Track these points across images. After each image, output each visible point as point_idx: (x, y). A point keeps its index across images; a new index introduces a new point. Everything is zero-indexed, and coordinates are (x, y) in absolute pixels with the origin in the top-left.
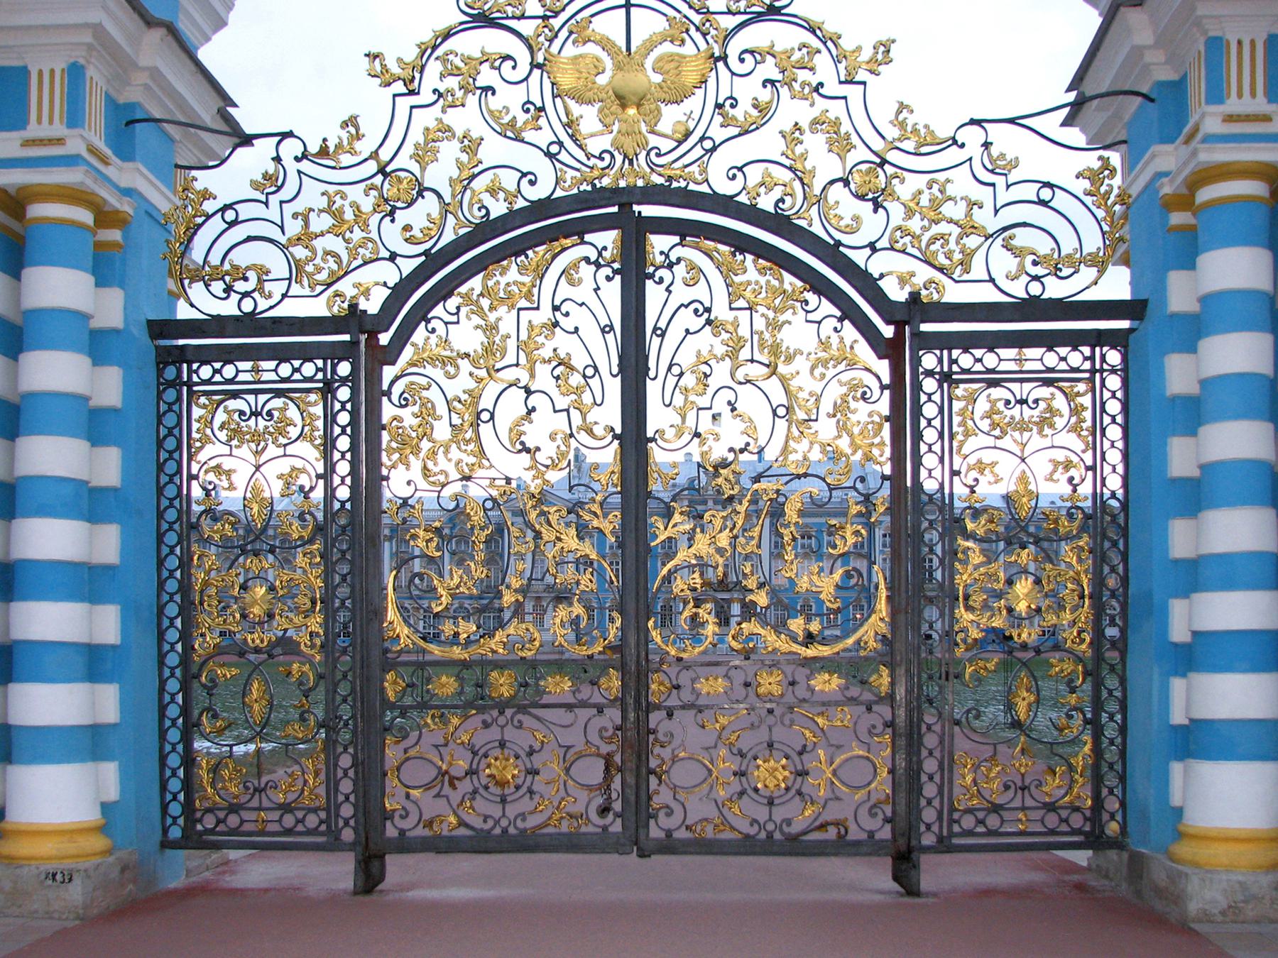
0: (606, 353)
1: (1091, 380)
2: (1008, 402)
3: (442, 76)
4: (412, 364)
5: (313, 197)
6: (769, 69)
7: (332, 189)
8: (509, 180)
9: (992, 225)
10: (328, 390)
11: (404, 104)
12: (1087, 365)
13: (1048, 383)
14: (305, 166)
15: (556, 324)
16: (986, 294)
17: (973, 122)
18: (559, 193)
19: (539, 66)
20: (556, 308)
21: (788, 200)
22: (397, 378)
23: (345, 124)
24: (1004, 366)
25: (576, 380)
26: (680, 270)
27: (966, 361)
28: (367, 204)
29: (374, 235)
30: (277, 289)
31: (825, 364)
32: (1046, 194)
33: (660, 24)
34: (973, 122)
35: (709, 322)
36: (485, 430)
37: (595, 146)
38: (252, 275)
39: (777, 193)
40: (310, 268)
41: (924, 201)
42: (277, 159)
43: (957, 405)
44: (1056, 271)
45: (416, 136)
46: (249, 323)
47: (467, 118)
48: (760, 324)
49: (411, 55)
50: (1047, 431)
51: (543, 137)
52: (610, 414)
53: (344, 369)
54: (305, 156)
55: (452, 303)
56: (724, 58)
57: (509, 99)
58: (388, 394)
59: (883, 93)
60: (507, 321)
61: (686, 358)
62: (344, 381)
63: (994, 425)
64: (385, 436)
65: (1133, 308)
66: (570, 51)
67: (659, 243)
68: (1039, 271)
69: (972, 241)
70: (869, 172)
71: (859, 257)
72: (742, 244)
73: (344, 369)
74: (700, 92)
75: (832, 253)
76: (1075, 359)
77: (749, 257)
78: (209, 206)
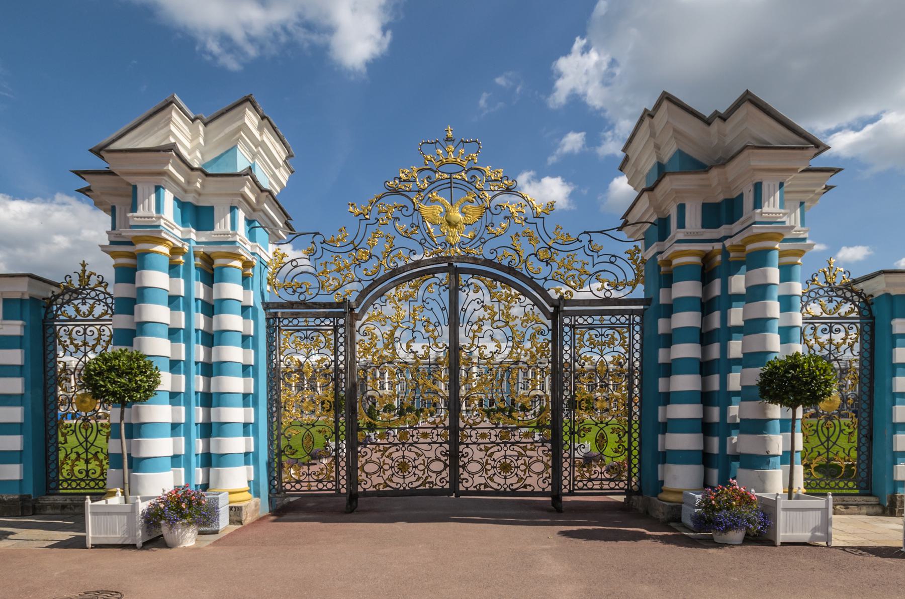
0: (443, 317)
2: (596, 335)
7: (335, 255)
9: (591, 270)
10: (335, 331)
11: (364, 223)
13: (611, 328)
14: (325, 245)
16: (588, 296)
17: (585, 232)
18: (425, 258)
22: (363, 325)
24: (595, 322)
25: (431, 328)
26: (472, 287)
27: (581, 321)
31: (527, 321)
32: (613, 259)
34: (585, 232)
35: (483, 306)
39: (509, 259)
41: (566, 262)
43: (577, 336)
44: (616, 288)
46: (303, 304)
48: (502, 307)
51: (419, 237)
52: (445, 340)
53: (341, 321)
54: (324, 242)
55: (383, 298)
58: (358, 331)
61: (474, 318)
62: (342, 326)
64: (357, 347)
65: (646, 301)
67: (463, 277)
69: (584, 277)
71: (540, 283)
72: (496, 278)
75: (530, 281)
76: (623, 320)
77: (499, 283)
78: (286, 260)
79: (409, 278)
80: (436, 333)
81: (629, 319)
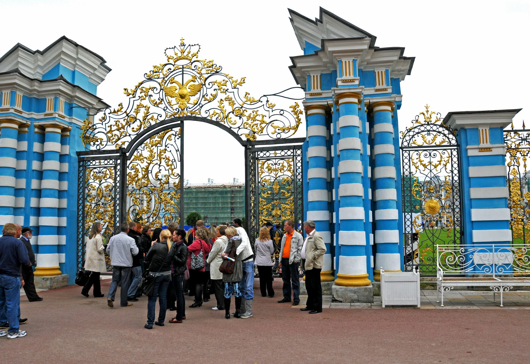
0: (177, 156)
1: (293, 158)
3: (141, 93)
4: (133, 160)
5: (112, 122)
6: (216, 87)
8: (155, 116)
11: (132, 100)
12: (292, 154)
14: (111, 115)
15: (166, 150)
16: (267, 138)
17: (264, 96)
18: (167, 119)
19: (162, 89)
20: (166, 146)
21: (219, 117)
23: (119, 105)
24: (271, 155)
25: (170, 163)
28: (124, 123)
29: (126, 130)
30: (104, 143)
32: (282, 112)
33: (191, 78)
34: (264, 96)
36: (150, 175)
37: (175, 107)
38: (99, 140)
40: (111, 139)
42: (105, 114)
45: (135, 107)
47: (146, 102)
49: (134, 88)
50: (282, 171)
52: (178, 171)
54: (111, 113)
55: (143, 145)
56: (205, 85)
57: (155, 97)
58: (128, 167)
59: (243, 90)
60: (155, 149)
63: (269, 170)
66: (169, 85)
68: (280, 131)
70: (239, 110)
71: (235, 131)
73: (119, 161)
74: (199, 93)
76: (289, 153)
79: (157, 133)
80: (173, 167)
81: (293, 153)
